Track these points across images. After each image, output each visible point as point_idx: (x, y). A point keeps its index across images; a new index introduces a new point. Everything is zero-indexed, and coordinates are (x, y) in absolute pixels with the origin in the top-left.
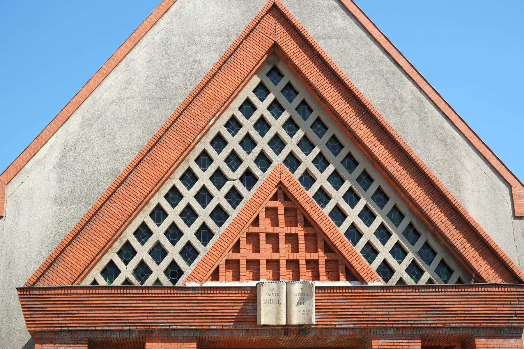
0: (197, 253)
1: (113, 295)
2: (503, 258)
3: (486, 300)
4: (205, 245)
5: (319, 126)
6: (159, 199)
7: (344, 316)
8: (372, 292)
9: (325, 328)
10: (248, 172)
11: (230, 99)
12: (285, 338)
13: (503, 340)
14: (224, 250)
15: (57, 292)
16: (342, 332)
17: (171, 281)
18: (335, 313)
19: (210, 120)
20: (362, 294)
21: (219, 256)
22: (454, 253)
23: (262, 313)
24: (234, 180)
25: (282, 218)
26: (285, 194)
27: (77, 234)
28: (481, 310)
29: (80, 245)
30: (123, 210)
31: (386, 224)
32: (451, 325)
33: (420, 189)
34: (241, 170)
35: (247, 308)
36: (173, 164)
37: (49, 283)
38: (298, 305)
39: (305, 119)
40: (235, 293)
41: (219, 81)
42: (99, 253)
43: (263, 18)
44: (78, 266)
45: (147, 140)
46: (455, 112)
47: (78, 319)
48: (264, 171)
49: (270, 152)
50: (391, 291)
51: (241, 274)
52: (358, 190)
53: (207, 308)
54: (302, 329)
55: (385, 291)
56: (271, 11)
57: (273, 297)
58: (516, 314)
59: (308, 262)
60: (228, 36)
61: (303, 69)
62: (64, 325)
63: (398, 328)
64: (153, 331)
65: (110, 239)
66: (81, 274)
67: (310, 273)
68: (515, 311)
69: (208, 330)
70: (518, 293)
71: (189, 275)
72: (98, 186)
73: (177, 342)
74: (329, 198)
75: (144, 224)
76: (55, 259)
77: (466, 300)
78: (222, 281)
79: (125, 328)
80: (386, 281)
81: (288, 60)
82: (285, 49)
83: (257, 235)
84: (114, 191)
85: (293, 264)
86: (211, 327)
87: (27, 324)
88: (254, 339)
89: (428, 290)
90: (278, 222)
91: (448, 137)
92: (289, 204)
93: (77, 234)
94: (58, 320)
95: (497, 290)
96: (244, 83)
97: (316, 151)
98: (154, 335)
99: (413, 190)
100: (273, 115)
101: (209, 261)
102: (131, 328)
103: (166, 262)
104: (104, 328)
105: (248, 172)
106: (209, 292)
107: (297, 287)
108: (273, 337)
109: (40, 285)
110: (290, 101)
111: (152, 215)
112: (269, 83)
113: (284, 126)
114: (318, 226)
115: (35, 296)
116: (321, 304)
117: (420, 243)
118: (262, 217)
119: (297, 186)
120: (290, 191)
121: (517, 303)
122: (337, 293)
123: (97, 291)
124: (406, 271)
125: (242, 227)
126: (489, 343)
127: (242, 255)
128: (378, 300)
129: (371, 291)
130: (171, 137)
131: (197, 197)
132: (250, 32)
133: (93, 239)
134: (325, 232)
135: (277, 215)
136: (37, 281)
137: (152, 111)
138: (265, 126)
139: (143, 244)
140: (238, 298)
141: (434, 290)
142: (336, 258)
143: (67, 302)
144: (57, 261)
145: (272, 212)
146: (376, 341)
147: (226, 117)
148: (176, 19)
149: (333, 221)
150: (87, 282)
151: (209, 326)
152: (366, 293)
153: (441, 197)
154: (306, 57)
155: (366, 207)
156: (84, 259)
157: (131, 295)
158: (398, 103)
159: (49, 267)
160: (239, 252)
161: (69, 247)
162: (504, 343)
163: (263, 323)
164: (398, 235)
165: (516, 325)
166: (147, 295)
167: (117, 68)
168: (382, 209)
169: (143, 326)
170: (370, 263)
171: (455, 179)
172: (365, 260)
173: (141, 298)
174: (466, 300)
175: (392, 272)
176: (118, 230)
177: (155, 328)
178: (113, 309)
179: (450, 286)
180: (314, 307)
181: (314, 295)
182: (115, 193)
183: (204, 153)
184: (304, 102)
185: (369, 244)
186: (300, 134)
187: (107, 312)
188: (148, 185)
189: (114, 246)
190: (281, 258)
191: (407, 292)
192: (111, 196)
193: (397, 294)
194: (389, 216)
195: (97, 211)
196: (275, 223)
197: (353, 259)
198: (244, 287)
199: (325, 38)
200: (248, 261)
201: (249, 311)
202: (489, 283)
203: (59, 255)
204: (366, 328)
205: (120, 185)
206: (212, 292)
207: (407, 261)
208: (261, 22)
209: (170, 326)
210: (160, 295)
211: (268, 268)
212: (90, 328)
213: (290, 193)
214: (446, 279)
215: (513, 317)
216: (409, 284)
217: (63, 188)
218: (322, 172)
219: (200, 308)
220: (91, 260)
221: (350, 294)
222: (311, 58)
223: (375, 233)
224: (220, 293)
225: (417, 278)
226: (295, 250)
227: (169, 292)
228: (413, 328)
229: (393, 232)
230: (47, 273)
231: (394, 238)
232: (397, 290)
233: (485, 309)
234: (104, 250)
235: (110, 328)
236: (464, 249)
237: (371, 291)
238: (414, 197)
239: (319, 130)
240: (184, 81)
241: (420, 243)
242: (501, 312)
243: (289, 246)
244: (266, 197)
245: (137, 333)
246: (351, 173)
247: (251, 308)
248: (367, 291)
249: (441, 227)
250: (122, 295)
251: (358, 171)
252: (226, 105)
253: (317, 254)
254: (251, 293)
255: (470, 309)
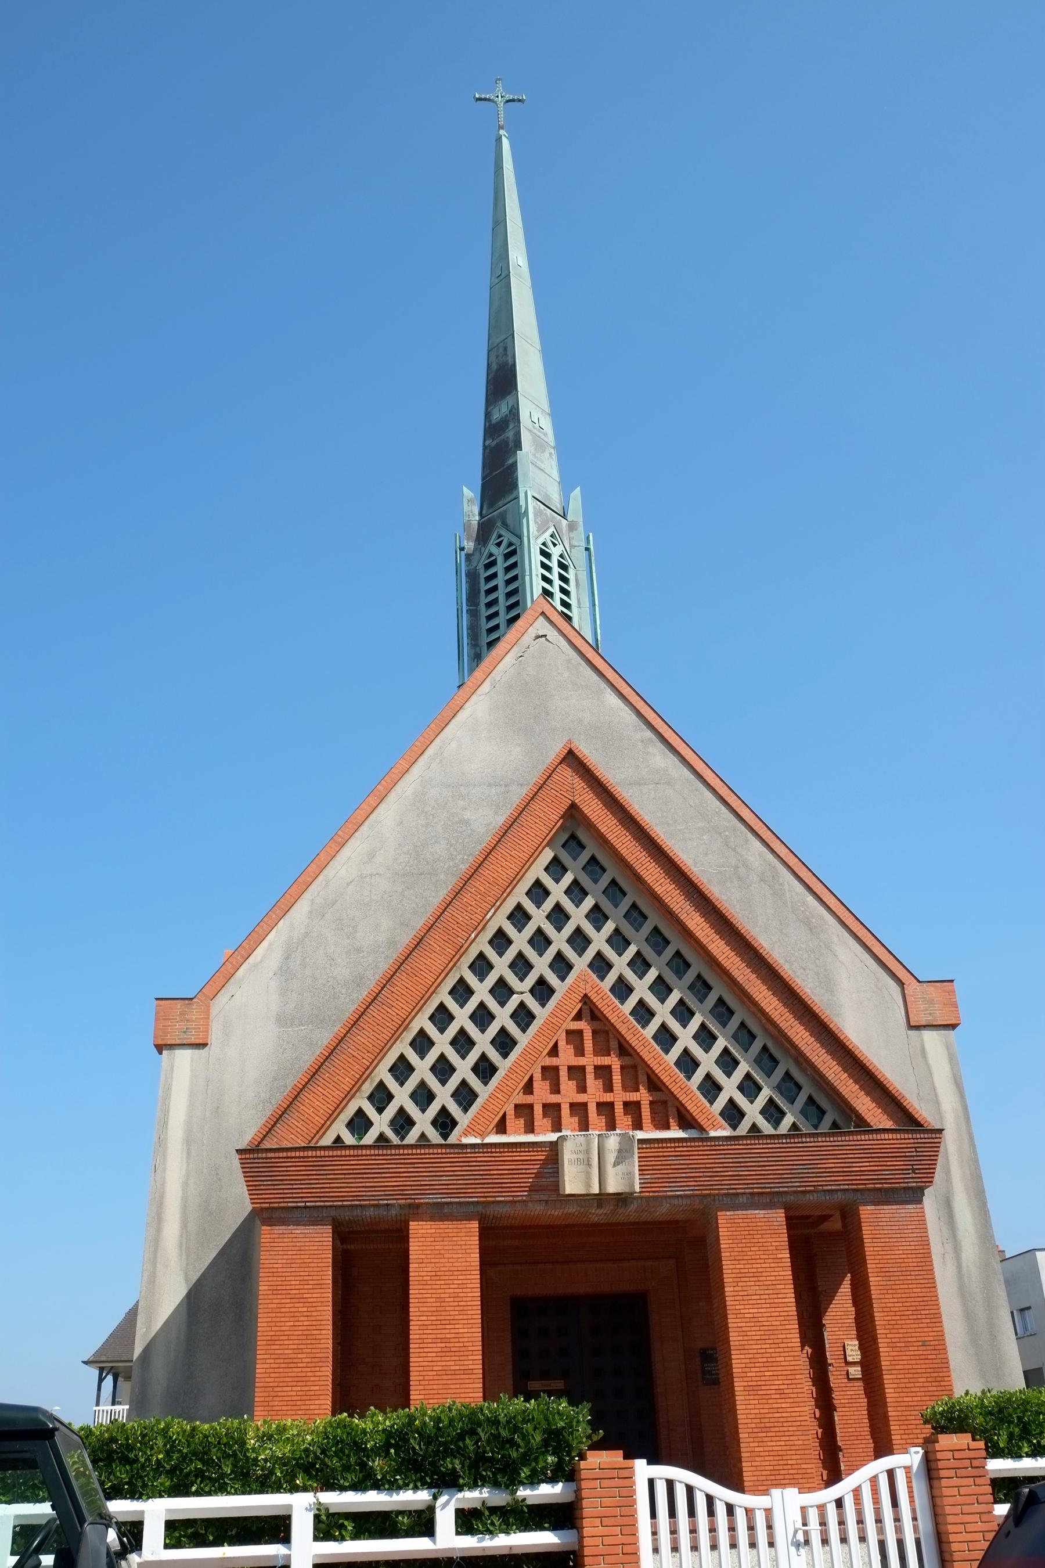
0: (475, 1096)
1: (364, 1158)
2: (893, 1092)
3: (871, 1151)
4: (486, 1084)
5: (636, 914)
6: (422, 1021)
7: (678, 1180)
8: (715, 1146)
9: (652, 1197)
10: (541, 982)
11: (515, 882)
12: (597, 1211)
13: (898, 1207)
14: (512, 1091)
15: (289, 1154)
16: (676, 1202)
17: (441, 1134)
18: (666, 1176)
19: (488, 912)
20: (701, 1148)
21: (505, 1100)
22: (825, 1086)
23: (567, 1178)
24: (522, 993)
25: (588, 1044)
26: (591, 1011)
27: (314, 1074)
28: (865, 1166)
29: (319, 1088)
30: (375, 1039)
31: (731, 1049)
32: (825, 1188)
33: (776, 999)
34: (531, 980)
35: (546, 1171)
36: (440, 974)
37: (278, 1141)
38: (614, 1166)
39: (616, 906)
40: (529, 1151)
41: (499, 857)
42: (343, 1099)
43: (555, 769)
44: (317, 1118)
45: (406, 938)
46: (821, 882)
47: (318, 1190)
48: (562, 978)
49: (570, 953)
50: (741, 1142)
51: (535, 1124)
52: (691, 1002)
53: (492, 1172)
54: (621, 1199)
55: (733, 1143)
56: (567, 760)
57: (581, 1156)
58: (913, 1170)
59: (626, 1104)
60: (506, 786)
61: (611, 837)
62: (300, 1200)
63: (752, 1194)
64: (419, 1205)
65: (359, 1080)
66: (320, 1129)
67: (630, 1120)
68: (912, 1165)
69: (493, 1202)
70: (916, 1141)
71: (465, 1126)
72: (334, 998)
73: (452, 1221)
74: (652, 1014)
75: (402, 1058)
76: (286, 1110)
77: (845, 1152)
78: (510, 1135)
79: (381, 1202)
80: (734, 1127)
81: (590, 826)
82: (586, 810)
83: (556, 1069)
84: (363, 1013)
85: (606, 1109)
86: (498, 1199)
87: (251, 1199)
88: (556, 1213)
89: (792, 1141)
90: (583, 1050)
91: (813, 917)
92: (597, 1025)
93: (314, 1074)
94: (292, 1193)
95: (887, 1138)
96: (532, 859)
97: (632, 950)
98: (420, 1211)
99: (766, 1001)
100: (573, 901)
101: (492, 1106)
102: (389, 1202)
103: (434, 1109)
104: (353, 1203)
105: (541, 982)
106: (493, 1150)
107: (613, 1142)
108: (582, 1210)
109: (267, 1145)
110: (596, 881)
111: (412, 1044)
112: (565, 858)
113: (587, 916)
114: (638, 1054)
115: (260, 1161)
116: (646, 1163)
117: (779, 1073)
118: (562, 1044)
119: (608, 999)
120: (599, 1007)
121: (915, 1154)
122: (668, 1147)
123: (343, 1153)
124: (761, 1113)
125: (535, 1059)
126: (878, 1212)
127: (536, 1098)
128: (723, 1156)
129: (713, 1143)
130: (436, 937)
131: (473, 1017)
132: (539, 790)
133: (335, 1080)
134: (649, 1063)
135: (582, 1040)
136: (262, 1140)
137: (406, 893)
138: (562, 916)
139: (402, 1084)
140: (533, 1158)
141: (800, 1140)
142: (664, 1098)
143: (304, 1168)
144: (288, 1112)
145: (575, 1037)
146: (723, 1213)
147: (509, 906)
148: (435, 764)
149: (658, 1045)
150: (328, 1140)
151: (495, 1197)
152: (707, 1146)
153: (805, 1009)
154: (616, 821)
155: (703, 1026)
156: (324, 1108)
157: (389, 1157)
158: (742, 871)
159: (278, 1120)
160: (532, 1093)
161: (303, 1092)
162: (898, 1211)
163: (568, 1192)
164: (747, 1063)
165: (914, 1184)
166: (410, 1157)
167: (356, 834)
168: (724, 1027)
169: (406, 1199)
170: (711, 1103)
171: (825, 975)
172: (703, 1099)
173: (403, 1161)
174: (845, 1152)
175: (742, 1114)
176: (368, 1067)
177: (422, 1201)
178: (365, 1176)
179: (821, 1133)
180: (637, 1168)
181: (636, 1150)
182: (364, 1016)
183: (481, 956)
184: (613, 882)
185: (708, 1077)
186: (609, 927)
187: (357, 1180)
188: (407, 1004)
189: (363, 1088)
190: (589, 1100)
191: (763, 1144)
192: (358, 1020)
193: (749, 1147)
194: (735, 1037)
195: (340, 1042)
196: (580, 1052)
197: (687, 1099)
198: (541, 1142)
199: (640, 784)
200: (545, 1106)
201: (548, 1175)
202: (875, 1128)
203: (291, 1103)
204: (709, 1195)
205: (370, 1004)
206: (498, 1150)
207: (761, 1100)
208: (553, 775)
209: (441, 1198)
210: (427, 1156)
211: (572, 1115)
212: (335, 1203)
213: (600, 1010)
214: (815, 1121)
215: (909, 1174)
216: (766, 1133)
217: (287, 1003)
218: (641, 978)
219: (481, 1173)
220: (333, 1109)
221: (685, 1149)
222: (622, 822)
223: (716, 1062)
224: (508, 1152)
225: (776, 1123)
226: (609, 1088)
227: (440, 1151)
228: (774, 1193)
229: (741, 1060)
230: (275, 1128)
231: (743, 1068)
232: (749, 1142)
233: (871, 1164)
234: (350, 1094)
235: (362, 1203)
236: (839, 1081)
237: (713, 1143)
238: (767, 1011)
239: (635, 919)
240: (448, 850)
241: (779, 1073)
242: (893, 1168)
243: (599, 1083)
244: (566, 1016)
245: (398, 1209)
246: (680, 978)
247: (550, 1171)
248: (709, 1144)
249: (807, 1051)
250: (377, 1158)
251: (690, 976)
252: (508, 890)
253: (638, 1093)
254: (551, 1150)
255: (851, 1165)
